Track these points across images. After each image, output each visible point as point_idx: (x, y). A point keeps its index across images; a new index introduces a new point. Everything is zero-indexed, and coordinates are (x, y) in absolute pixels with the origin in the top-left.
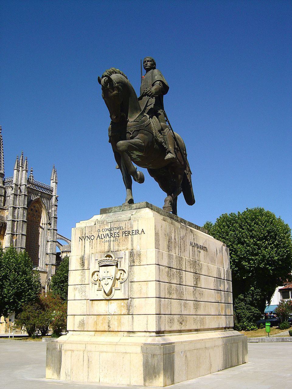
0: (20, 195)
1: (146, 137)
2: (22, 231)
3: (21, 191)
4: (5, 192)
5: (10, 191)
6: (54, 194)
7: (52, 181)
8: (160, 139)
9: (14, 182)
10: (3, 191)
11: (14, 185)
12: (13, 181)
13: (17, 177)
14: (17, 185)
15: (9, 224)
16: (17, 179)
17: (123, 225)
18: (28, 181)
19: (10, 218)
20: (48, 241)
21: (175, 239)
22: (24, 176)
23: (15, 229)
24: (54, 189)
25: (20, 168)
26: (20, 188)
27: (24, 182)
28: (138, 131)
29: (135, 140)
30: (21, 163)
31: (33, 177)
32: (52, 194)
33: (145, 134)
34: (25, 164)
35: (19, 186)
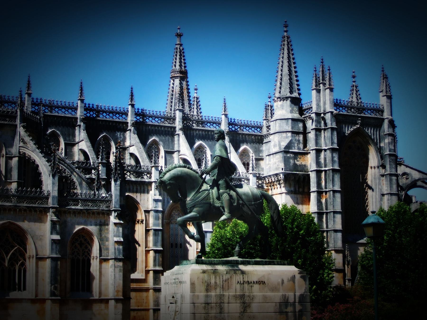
0: (325, 130)
1: (200, 209)
2: (333, 186)
3: (326, 124)
4: (305, 127)
5: (310, 125)
6: (386, 115)
7: (381, 94)
8: (218, 204)
9: (314, 110)
10: (301, 125)
11: (313, 116)
12: (312, 108)
13: (318, 101)
14: (318, 114)
15: (313, 176)
16: (318, 105)
17: (179, 276)
18: (337, 104)
19: (314, 167)
20: (383, 195)
21: (216, 283)
22: (328, 98)
23: (323, 184)
24: (385, 108)
25: (321, 85)
26: (324, 119)
27: (329, 108)
28: (194, 207)
29: (192, 214)
30: (321, 78)
31: (356, 87)
32: (382, 116)
33: (199, 207)
34: (328, 78)
35: (322, 115)
